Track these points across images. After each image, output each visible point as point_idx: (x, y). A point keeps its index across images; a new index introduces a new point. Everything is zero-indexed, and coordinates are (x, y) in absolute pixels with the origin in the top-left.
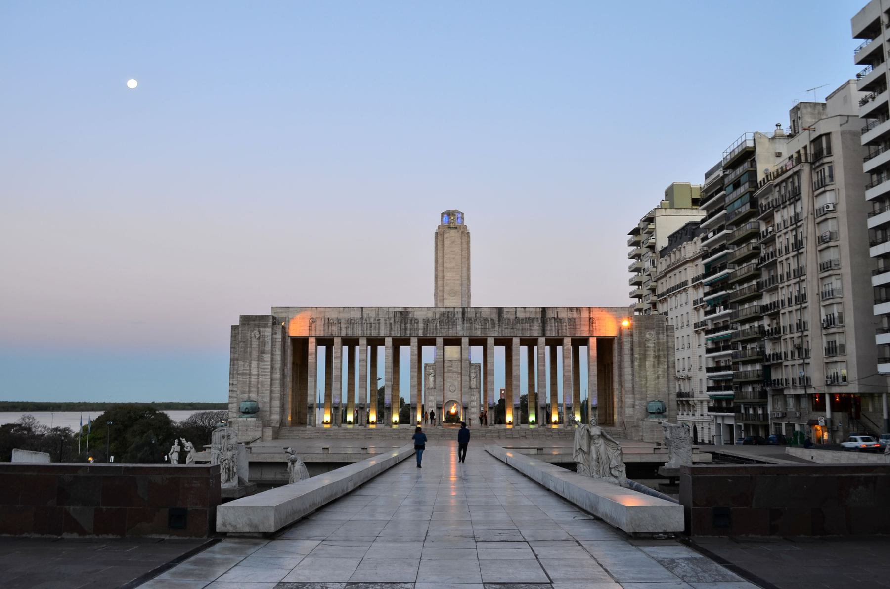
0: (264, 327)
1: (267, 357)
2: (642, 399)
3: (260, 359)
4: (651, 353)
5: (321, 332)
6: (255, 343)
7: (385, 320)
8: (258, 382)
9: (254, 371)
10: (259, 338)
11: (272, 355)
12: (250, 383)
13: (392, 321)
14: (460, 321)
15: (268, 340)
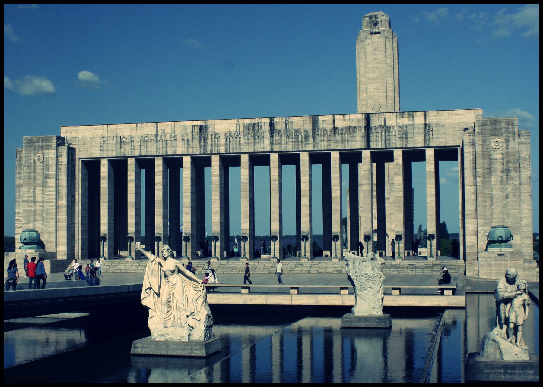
0: (48, 149)
1: (52, 182)
2: (485, 224)
3: (44, 184)
4: (498, 166)
5: (113, 153)
6: (39, 167)
7: (183, 136)
8: (43, 210)
9: (39, 198)
10: (43, 161)
11: (57, 179)
12: (35, 212)
13: (190, 137)
14: (267, 135)
15: (53, 163)
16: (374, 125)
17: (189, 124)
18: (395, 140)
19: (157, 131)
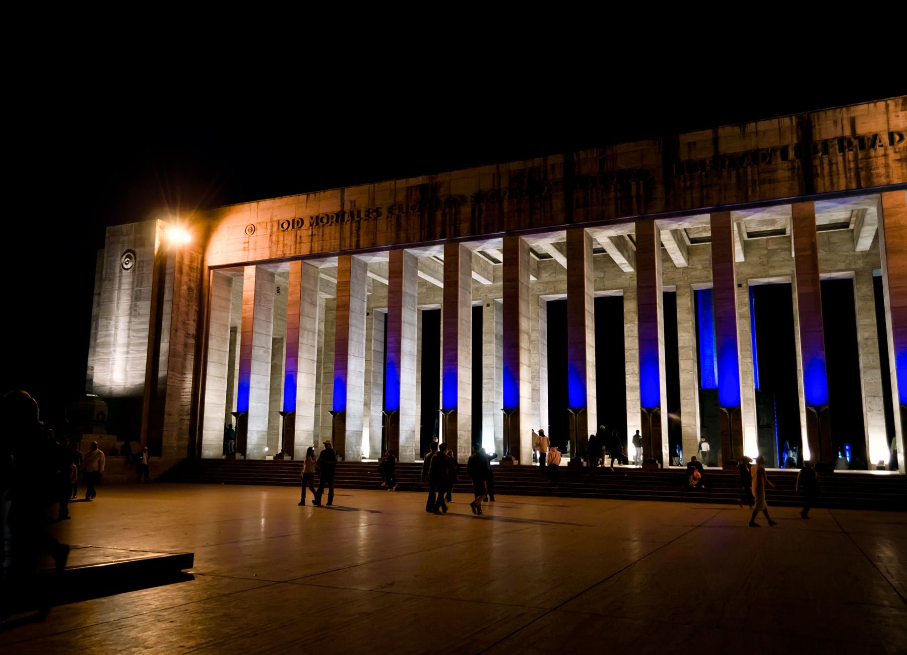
16: (825, 136)
17: (401, 183)
18: (887, 166)
19: (343, 205)
